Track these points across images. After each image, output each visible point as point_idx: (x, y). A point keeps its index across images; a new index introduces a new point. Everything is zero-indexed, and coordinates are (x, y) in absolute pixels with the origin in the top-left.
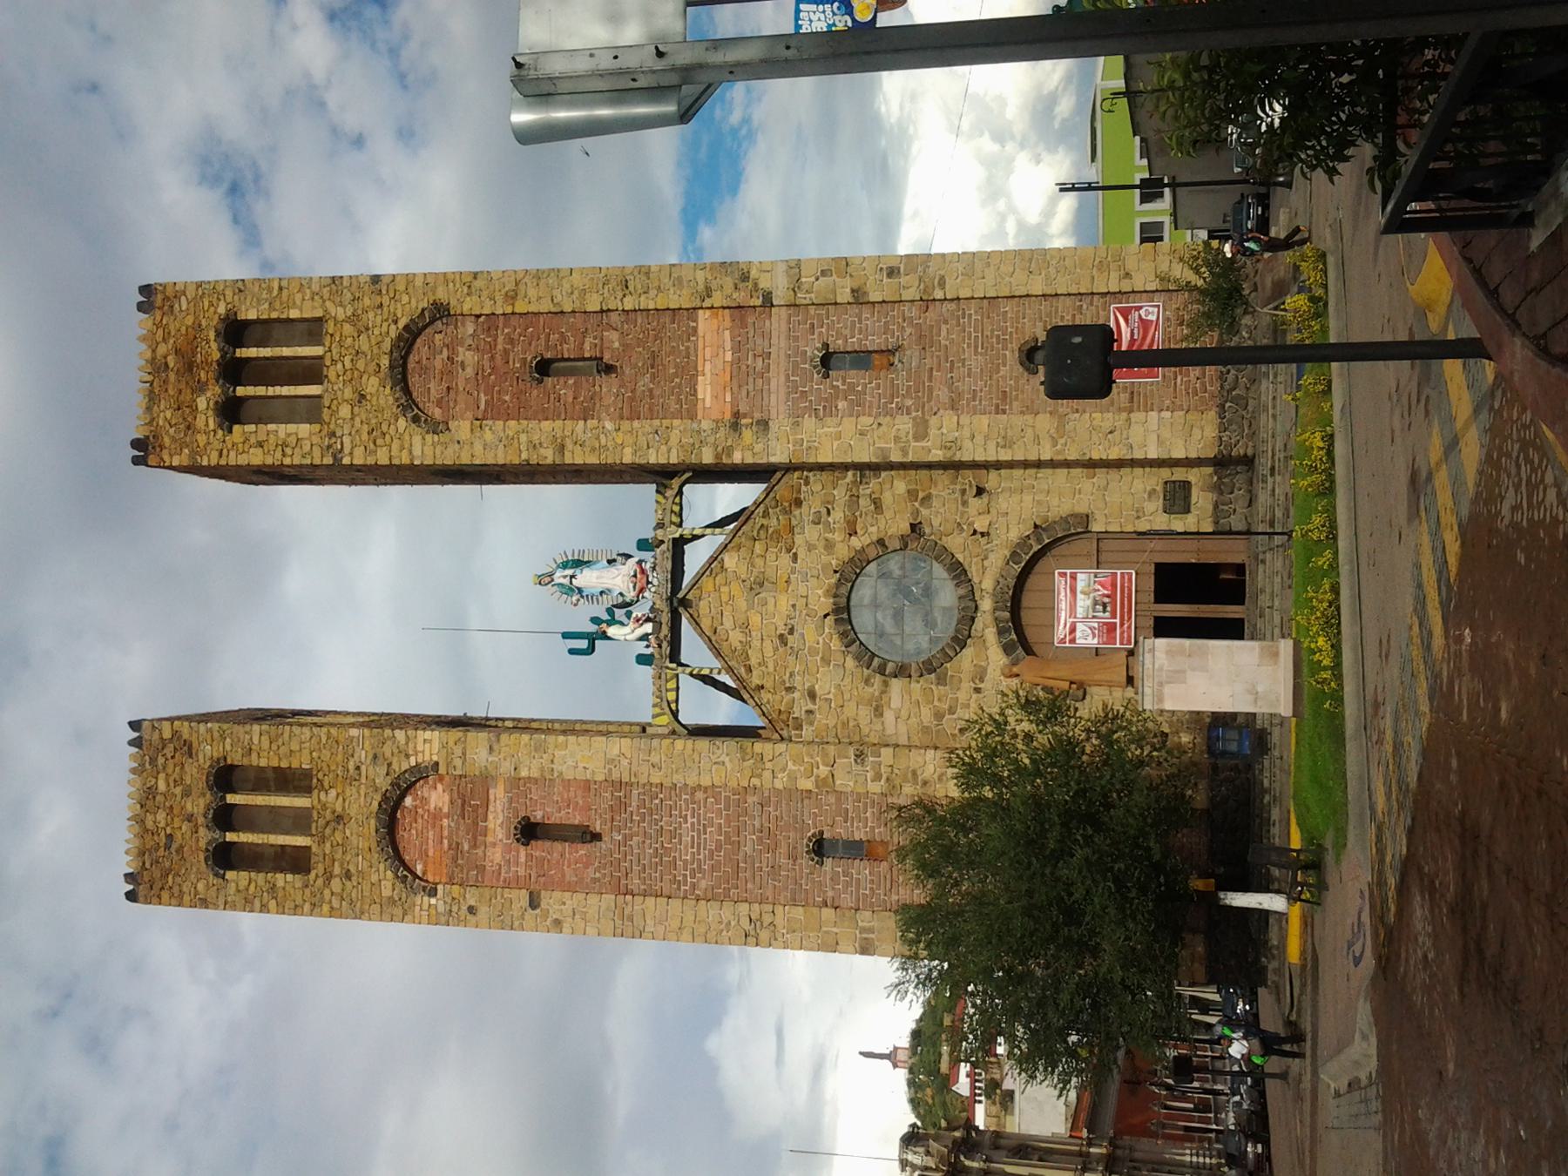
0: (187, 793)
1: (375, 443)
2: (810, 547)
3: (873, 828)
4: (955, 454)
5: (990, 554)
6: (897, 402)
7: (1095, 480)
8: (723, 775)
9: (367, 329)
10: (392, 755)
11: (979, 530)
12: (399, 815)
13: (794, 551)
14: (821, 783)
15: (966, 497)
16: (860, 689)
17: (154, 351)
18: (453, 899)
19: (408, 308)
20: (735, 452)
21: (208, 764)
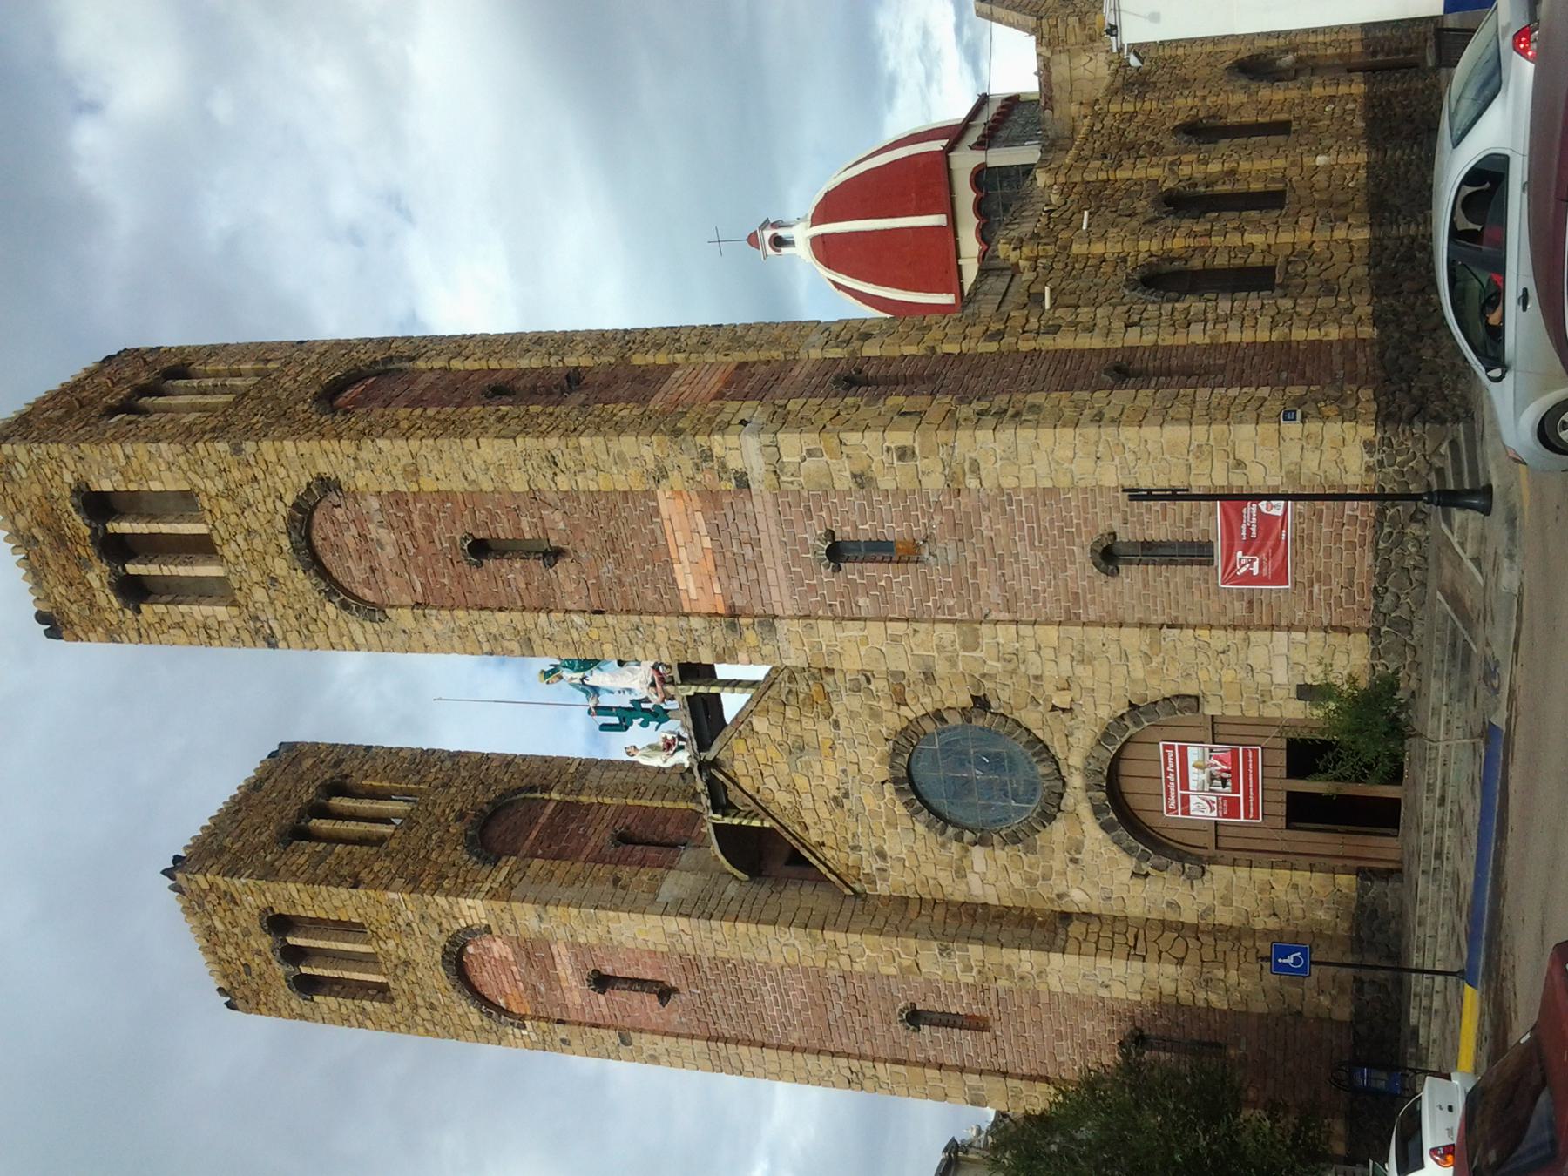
0: (246, 933)
1: (309, 630)
2: (853, 715)
10: (440, 916)
12: (465, 959)
13: (834, 717)
16: (936, 852)
17: (13, 522)
20: (740, 654)
21: (256, 912)
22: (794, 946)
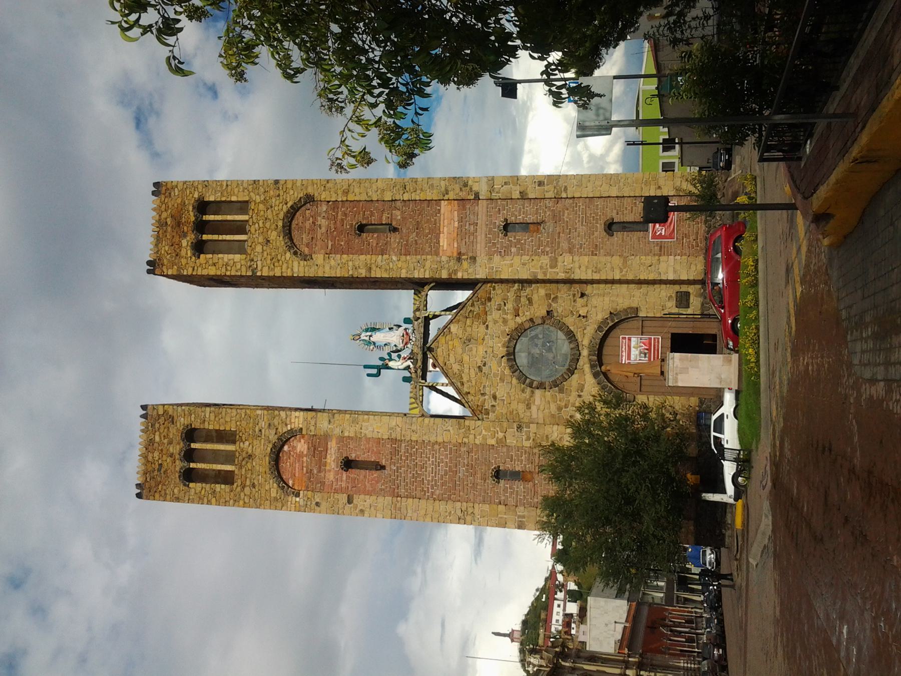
0: (170, 443)
1: (274, 265)
2: (495, 322)
3: (525, 465)
6: (542, 249)
7: (641, 290)
8: (449, 437)
9: (272, 207)
11: (582, 315)
12: (281, 455)
13: (487, 324)
14: (499, 441)
15: (575, 298)
17: (160, 216)
18: (308, 498)
19: (293, 197)
21: (182, 427)
22: (449, 431)
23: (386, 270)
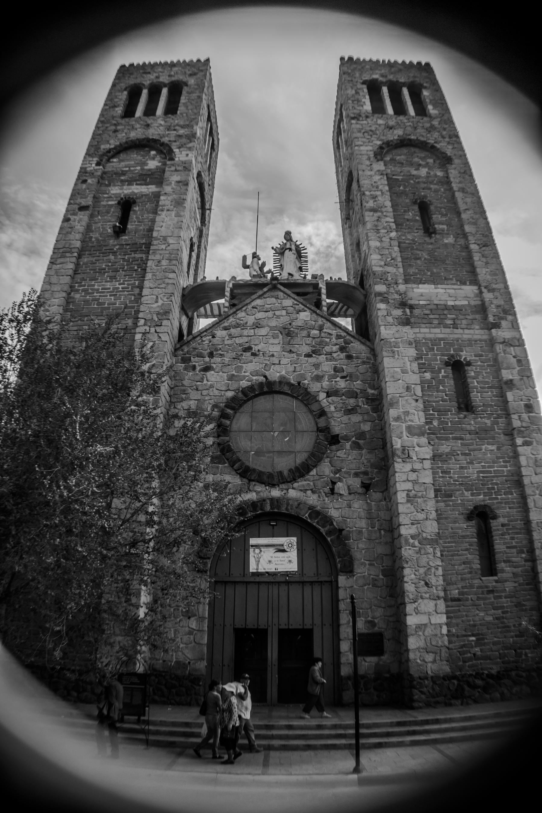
2: (317, 366)
4: (399, 457)
5: (317, 495)
7: (381, 577)
11: (336, 487)
13: (314, 355)
16: (211, 402)
22: (157, 302)
23: (376, 226)
